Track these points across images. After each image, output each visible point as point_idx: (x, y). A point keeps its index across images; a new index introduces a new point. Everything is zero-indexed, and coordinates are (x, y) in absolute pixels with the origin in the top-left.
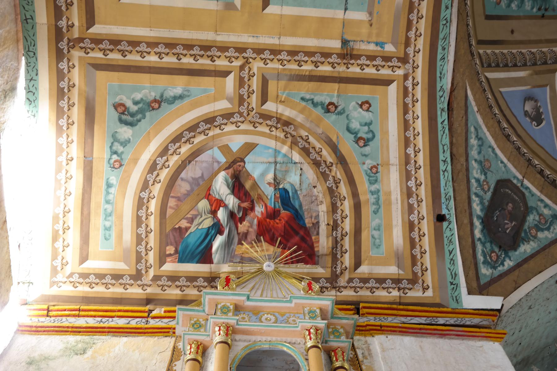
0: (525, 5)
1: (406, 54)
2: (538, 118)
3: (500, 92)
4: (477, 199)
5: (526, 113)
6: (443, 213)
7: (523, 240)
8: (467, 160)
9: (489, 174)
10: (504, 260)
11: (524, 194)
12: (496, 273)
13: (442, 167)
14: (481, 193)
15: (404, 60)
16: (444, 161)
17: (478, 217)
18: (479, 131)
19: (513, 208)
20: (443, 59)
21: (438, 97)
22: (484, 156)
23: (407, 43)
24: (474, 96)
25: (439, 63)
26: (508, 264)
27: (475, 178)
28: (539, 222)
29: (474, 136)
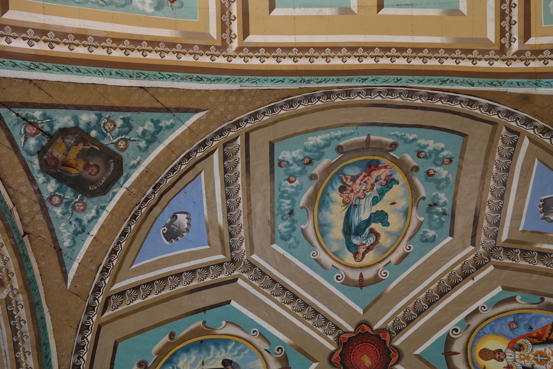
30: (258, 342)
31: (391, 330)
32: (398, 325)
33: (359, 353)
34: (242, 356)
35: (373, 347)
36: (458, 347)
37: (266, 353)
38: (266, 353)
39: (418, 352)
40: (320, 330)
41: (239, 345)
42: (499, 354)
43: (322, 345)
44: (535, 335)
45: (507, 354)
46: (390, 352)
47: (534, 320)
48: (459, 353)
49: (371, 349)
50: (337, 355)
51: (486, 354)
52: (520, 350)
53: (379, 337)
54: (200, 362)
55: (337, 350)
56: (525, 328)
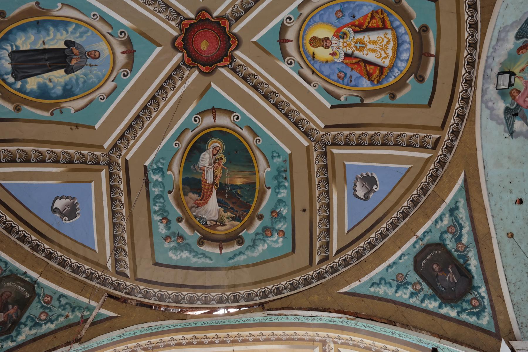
1: (320, 341)
2: (370, 181)
3: (348, 232)
4: (426, 302)
5: (366, 197)
6: (431, 348)
7: (466, 261)
8: (395, 302)
9: (409, 279)
10: (480, 294)
12: (488, 310)
13: (397, 336)
15: (324, 343)
16: (393, 334)
17: (440, 307)
18: (375, 281)
19: (438, 265)
20: (321, 320)
21: (347, 325)
22: (394, 280)
23: (313, 341)
24: (348, 283)
25: (324, 322)
27: (409, 298)
28: (454, 234)
29: (378, 289)
30: (99, 25)
31: (230, 18)
32: (237, 12)
33: (199, 38)
34: (84, 38)
35: (213, 34)
36: (291, 35)
37: (109, 36)
38: (109, 36)
39: (255, 39)
42: (326, 41)
44: (357, 23)
45: (333, 42)
46: (230, 39)
49: (211, 35)
50: (179, 40)
51: (315, 42)
52: (343, 38)
53: (219, 23)
54: (41, 42)
55: (180, 35)
56: (349, 17)
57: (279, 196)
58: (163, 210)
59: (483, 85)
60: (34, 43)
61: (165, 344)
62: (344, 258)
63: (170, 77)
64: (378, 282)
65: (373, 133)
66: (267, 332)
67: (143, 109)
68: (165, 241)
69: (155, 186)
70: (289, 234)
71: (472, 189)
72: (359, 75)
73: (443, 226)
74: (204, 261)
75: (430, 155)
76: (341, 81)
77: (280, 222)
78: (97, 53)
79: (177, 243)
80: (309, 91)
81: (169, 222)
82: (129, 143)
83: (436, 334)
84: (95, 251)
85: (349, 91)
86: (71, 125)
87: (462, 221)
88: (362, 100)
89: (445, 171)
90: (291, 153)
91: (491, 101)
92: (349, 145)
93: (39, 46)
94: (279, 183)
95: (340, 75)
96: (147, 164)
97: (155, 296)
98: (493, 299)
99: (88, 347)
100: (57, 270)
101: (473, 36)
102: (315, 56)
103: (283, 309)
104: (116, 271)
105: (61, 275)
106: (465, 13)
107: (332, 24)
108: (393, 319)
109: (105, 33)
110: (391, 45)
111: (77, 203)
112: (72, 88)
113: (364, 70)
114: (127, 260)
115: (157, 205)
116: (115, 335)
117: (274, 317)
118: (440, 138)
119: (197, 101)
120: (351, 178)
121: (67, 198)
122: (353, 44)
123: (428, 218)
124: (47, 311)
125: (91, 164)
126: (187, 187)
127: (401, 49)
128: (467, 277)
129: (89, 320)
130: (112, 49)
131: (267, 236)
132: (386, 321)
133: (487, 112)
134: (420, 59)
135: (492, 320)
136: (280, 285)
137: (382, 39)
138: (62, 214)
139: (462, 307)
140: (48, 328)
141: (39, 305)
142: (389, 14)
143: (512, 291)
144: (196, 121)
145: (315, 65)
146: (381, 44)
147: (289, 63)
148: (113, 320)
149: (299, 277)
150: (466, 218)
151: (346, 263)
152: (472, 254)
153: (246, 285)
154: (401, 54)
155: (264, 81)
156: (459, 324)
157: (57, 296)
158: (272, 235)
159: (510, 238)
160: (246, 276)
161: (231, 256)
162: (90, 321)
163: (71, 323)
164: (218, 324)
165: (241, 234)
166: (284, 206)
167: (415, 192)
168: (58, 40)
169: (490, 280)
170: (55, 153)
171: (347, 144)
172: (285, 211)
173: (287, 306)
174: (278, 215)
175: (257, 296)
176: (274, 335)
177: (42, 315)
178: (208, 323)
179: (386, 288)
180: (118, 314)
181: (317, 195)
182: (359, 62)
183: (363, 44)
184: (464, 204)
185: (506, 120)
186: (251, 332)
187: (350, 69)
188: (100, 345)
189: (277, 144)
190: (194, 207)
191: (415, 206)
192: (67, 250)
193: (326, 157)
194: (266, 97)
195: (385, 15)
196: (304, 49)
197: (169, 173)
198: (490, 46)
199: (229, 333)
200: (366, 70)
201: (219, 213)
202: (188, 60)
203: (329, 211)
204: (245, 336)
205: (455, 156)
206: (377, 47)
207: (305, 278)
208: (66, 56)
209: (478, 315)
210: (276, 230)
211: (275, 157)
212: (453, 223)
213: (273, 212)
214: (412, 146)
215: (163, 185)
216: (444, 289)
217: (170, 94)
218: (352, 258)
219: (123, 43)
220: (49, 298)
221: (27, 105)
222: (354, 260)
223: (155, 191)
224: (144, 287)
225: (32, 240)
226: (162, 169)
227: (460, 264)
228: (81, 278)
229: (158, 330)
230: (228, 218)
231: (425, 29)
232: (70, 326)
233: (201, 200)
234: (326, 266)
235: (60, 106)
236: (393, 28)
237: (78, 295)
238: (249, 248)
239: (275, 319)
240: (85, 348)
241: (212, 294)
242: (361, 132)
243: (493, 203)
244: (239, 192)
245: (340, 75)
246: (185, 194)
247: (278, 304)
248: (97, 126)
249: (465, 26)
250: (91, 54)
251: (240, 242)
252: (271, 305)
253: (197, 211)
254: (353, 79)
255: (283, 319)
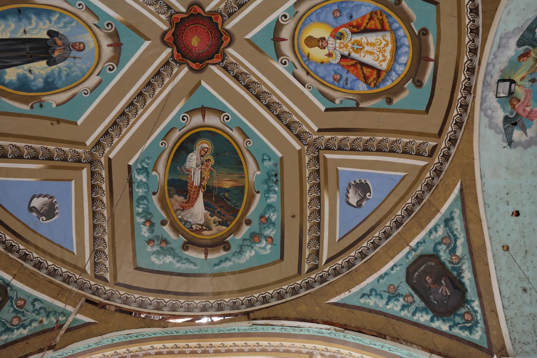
0: (273, 202)
1: (307, 353)
2: (363, 188)
3: (339, 240)
5: (359, 205)
7: (460, 274)
8: (385, 315)
11: (421, 257)
12: (481, 324)
13: (387, 350)
14: (413, 308)
16: (382, 347)
17: (432, 320)
18: (365, 292)
19: (431, 277)
20: (308, 331)
21: (335, 337)
22: (385, 291)
23: (300, 352)
24: (338, 293)
25: (312, 333)
26: (477, 306)
27: (401, 310)
28: (448, 245)
30: (85, 16)
31: (223, 13)
32: (230, 8)
33: (190, 34)
34: (69, 29)
36: (286, 33)
37: (95, 28)
38: (95, 28)
39: (248, 36)
40: (151, 8)
41: (65, 17)
42: (322, 42)
43: (154, 23)
44: (355, 24)
45: (329, 42)
46: (222, 35)
47: (356, 8)
48: (287, 40)
49: (202, 30)
50: (169, 35)
51: (311, 42)
52: (340, 39)
54: (22, 31)
55: (170, 29)
56: (347, 17)
57: (269, 201)
58: (146, 212)
59: (482, 93)
60: (15, 31)
61: (144, 352)
62: (334, 267)
63: (158, 73)
64: (369, 293)
65: (368, 138)
66: (252, 342)
67: (129, 106)
68: (148, 244)
69: (138, 187)
70: (278, 241)
71: (468, 200)
72: (355, 78)
73: (438, 236)
74: (188, 266)
75: (426, 163)
76: (336, 83)
77: (269, 228)
78: (82, 45)
79: (161, 247)
80: (303, 92)
81: (152, 225)
82: (113, 141)
83: (426, 348)
84: (73, 253)
85: (344, 94)
86: (52, 120)
87: (457, 232)
88: (358, 104)
89: (441, 180)
90: (282, 157)
91: (490, 109)
92: (342, 150)
93: (20, 35)
94: (269, 187)
95: (336, 77)
96: (131, 163)
97: (135, 302)
98: (487, 313)
99: (62, 355)
100: (32, 273)
101: (473, 41)
102: (310, 57)
103: (269, 319)
104: (95, 275)
105: (36, 278)
106: (467, 18)
107: (329, 24)
108: (382, 332)
109: (91, 24)
110: (389, 48)
111: (55, 202)
112: (54, 81)
113: (361, 73)
114: (107, 263)
115: (141, 206)
116: (92, 342)
117: (259, 327)
118: (437, 145)
119: (186, 100)
120: (343, 184)
121: (45, 196)
122: (350, 45)
123: (423, 228)
124: (19, 315)
125: (72, 162)
126: (172, 188)
127: (399, 52)
128: (461, 290)
129: (65, 326)
130: (98, 41)
131: (255, 242)
132: (375, 334)
133: (485, 120)
134: (419, 63)
135: (485, 336)
136: (267, 294)
137: (381, 41)
138: (40, 214)
139: (454, 321)
140: (21, 333)
141: (12, 310)
142: (388, 16)
143: (506, 306)
144: (184, 120)
145: (310, 66)
146: (379, 47)
147: (283, 62)
148: (90, 326)
149: (287, 286)
150: (461, 228)
151: (336, 272)
152: (466, 267)
153: (231, 293)
154: (399, 57)
155: (256, 81)
156: (451, 338)
157: (31, 300)
158: (260, 242)
159: (506, 251)
160: (231, 283)
161: (217, 262)
162: (65, 327)
163: (45, 328)
164: (201, 333)
165: (227, 239)
166: (274, 211)
167: (409, 201)
168: (41, 29)
169: (483, 293)
170: (33, 148)
171: (341, 149)
172: (274, 217)
173: (273, 316)
174: (267, 221)
175: (242, 304)
176: (258, 346)
177: (14, 320)
178: (190, 331)
179: (376, 300)
180: (96, 320)
181: (308, 201)
182: (355, 64)
183: (360, 46)
184: (459, 215)
185: (505, 129)
186: (235, 342)
187: (346, 71)
188: (75, 352)
189: (268, 147)
190: (179, 209)
191: (409, 215)
192: (44, 252)
193: (318, 162)
194: (258, 97)
195: (384, 16)
196: (299, 49)
197: (154, 173)
198: (490, 52)
199: (212, 343)
200: (363, 73)
201: (205, 216)
202: (178, 56)
203: (320, 218)
204: (228, 346)
205: (451, 165)
206: (375, 49)
207: (293, 287)
208: (49, 47)
209: (470, 330)
210: (265, 236)
211: (265, 160)
212: (448, 234)
213: (261, 217)
214: (408, 153)
215: (147, 186)
216: (436, 302)
217: (158, 91)
218: (342, 267)
219: (110, 35)
220: (23, 302)
221: (5, 97)
222: (344, 270)
223: (139, 192)
224: (124, 293)
225: (6, 240)
226: (147, 169)
227: (454, 277)
228: (57, 281)
229: (136, 338)
230: (215, 223)
231: (424, 32)
232: (44, 332)
233: (186, 203)
234: (315, 275)
235: (40, 99)
236: (392, 30)
237: (53, 300)
238: (236, 254)
239: (260, 329)
240: (59, 355)
241: (195, 301)
242: (355, 137)
243: (489, 215)
244: (227, 196)
245: (336, 77)
246: (171, 196)
247: (265, 313)
248: (79, 122)
249: (466, 31)
250: (76, 46)
251: (227, 247)
252: (257, 314)
253: (182, 214)
254: (349, 82)
255: (269, 330)
